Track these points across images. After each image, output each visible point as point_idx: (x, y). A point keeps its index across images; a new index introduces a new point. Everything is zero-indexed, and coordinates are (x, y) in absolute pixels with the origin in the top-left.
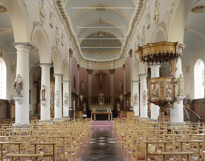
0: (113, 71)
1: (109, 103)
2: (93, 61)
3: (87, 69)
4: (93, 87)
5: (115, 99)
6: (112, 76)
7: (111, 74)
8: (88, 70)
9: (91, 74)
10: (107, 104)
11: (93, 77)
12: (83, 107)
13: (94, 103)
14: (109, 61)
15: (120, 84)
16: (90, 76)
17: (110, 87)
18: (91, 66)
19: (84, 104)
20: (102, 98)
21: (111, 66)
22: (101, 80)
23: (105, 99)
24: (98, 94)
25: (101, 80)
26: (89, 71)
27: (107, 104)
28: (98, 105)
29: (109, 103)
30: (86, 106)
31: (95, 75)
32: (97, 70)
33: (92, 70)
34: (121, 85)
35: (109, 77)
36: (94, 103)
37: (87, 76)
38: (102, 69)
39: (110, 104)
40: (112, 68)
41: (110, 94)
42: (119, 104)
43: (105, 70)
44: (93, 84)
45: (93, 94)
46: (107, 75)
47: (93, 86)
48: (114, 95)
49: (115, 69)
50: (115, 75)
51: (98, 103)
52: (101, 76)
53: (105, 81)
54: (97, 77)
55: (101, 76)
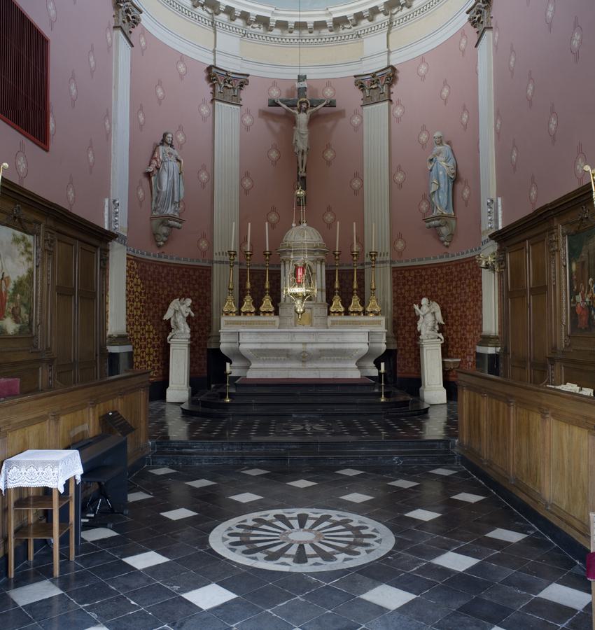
0: (380, 84)
1: (355, 300)
2: (245, 16)
3: (209, 69)
4: (245, 192)
5: (394, 270)
6: (376, 118)
7: (368, 101)
8: (212, 74)
9: (235, 101)
10: (346, 303)
11: (246, 128)
12: (168, 327)
13: (248, 300)
14: (359, 17)
15: (440, 159)
16: (228, 118)
17: (359, 192)
18: (232, 52)
19: (175, 304)
20: (304, 258)
21: (371, 52)
22: (302, 144)
23: (330, 275)
24: (278, 238)
25: (302, 144)
26: (224, 84)
27: (346, 303)
28: (276, 313)
29: (355, 300)
30: (189, 320)
31: (264, 114)
32: (275, 83)
33: (243, 81)
34: (443, 166)
35: (358, 129)
36: (248, 300)
37: (205, 110)
38: (312, 74)
39: (363, 303)
40: (377, 64)
41: (361, 242)
42: (436, 307)
43: (328, 83)
44: (245, 174)
45: (242, 241)
46: (341, 114)
47: (247, 183)
48: (393, 244)
49: (393, 69)
50: (398, 111)
51: (276, 301)
52: (303, 118)
53: (329, 155)
54: (276, 126)
55: (303, 118)
